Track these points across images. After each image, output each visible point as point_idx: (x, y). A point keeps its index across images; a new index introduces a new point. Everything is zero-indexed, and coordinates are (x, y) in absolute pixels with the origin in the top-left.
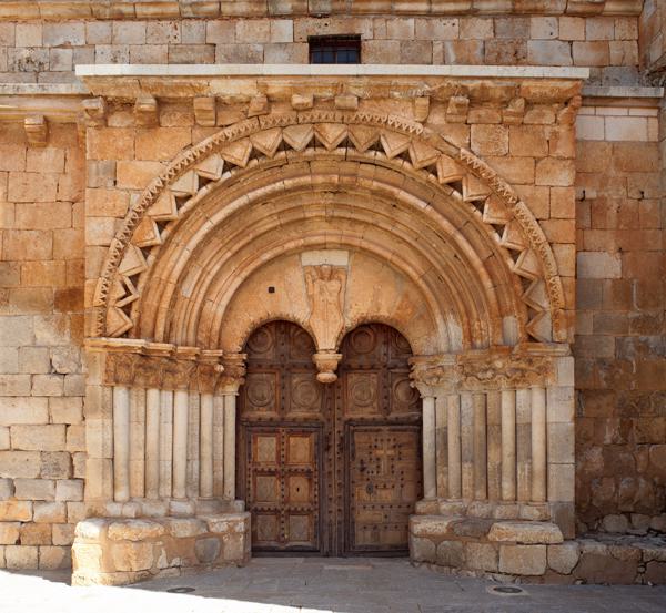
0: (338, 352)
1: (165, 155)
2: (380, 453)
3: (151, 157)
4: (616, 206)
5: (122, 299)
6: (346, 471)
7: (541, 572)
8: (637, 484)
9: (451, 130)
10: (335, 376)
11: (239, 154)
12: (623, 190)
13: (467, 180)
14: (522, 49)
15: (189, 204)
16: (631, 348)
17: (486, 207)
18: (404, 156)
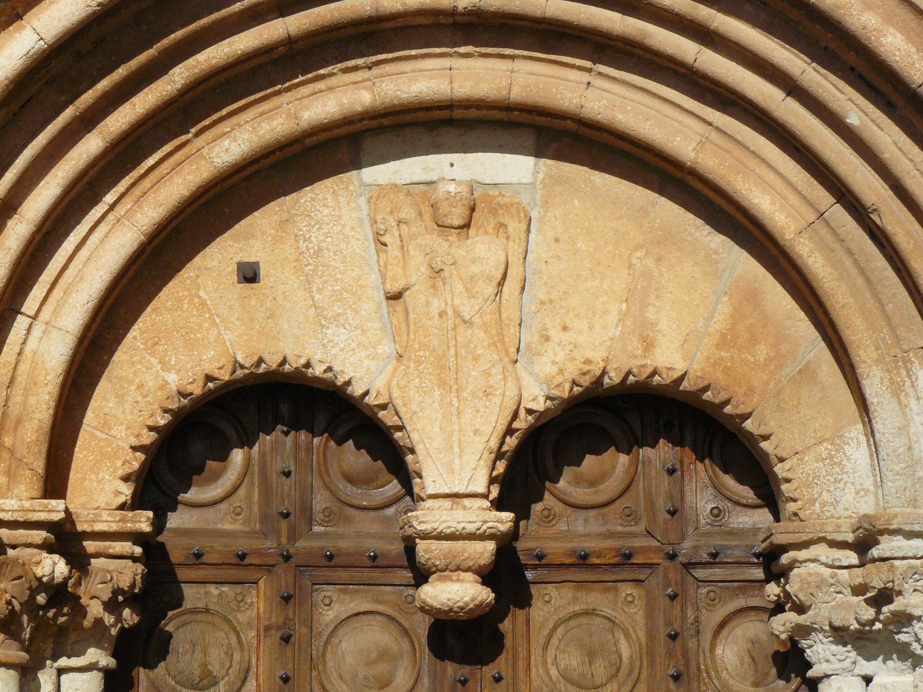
0: (499, 505)
10: (486, 595)
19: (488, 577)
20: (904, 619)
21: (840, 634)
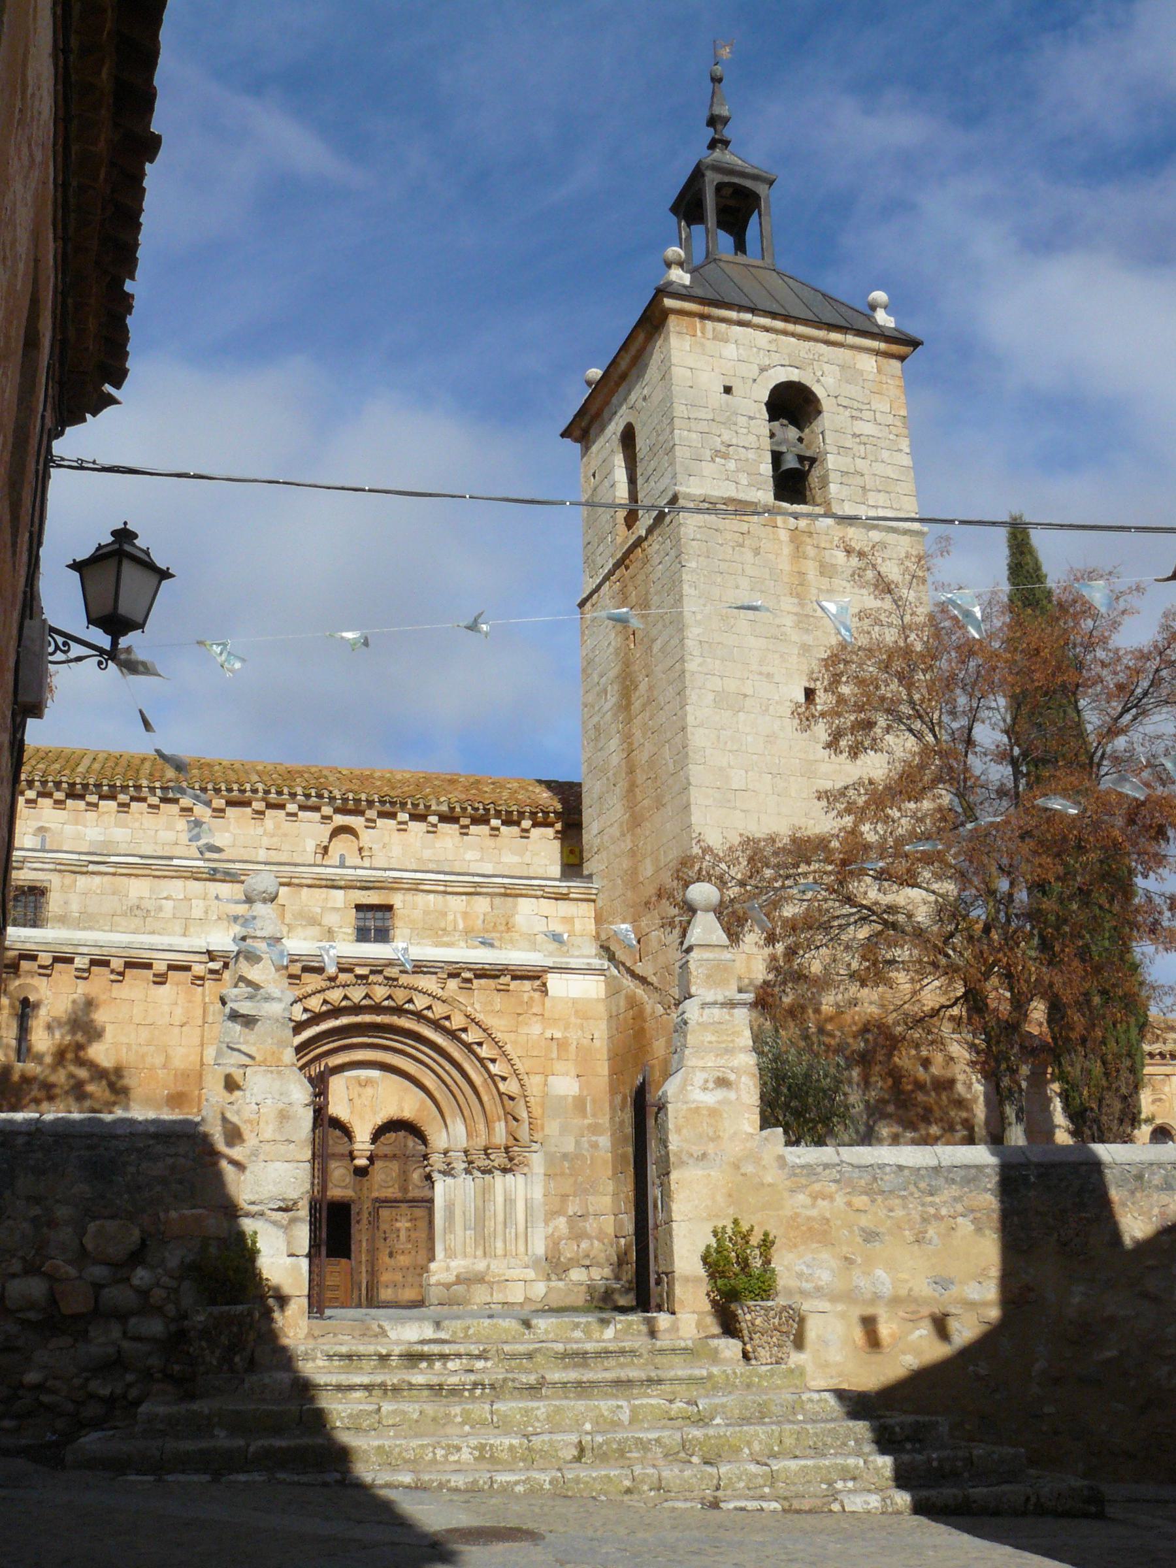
2: (398, 1225)
4: (575, 1043)
6: (372, 1240)
7: (521, 1300)
8: (592, 1244)
12: (580, 1032)
16: (586, 1146)
17: (484, 1046)
18: (429, 1008)
19: (368, 1159)
20: (453, 1168)
21: (440, 1172)
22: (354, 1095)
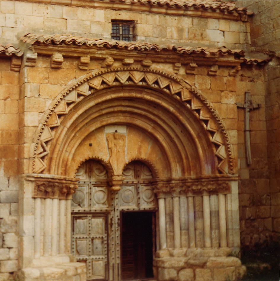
1: (63, 82)
3: (56, 83)
5: (40, 153)
9: (188, 77)
11: (97, 83)
13: (194, 100)
14: (204, 33)
15: (72, 106)
17: (201, 112)
22: (112, 145)
